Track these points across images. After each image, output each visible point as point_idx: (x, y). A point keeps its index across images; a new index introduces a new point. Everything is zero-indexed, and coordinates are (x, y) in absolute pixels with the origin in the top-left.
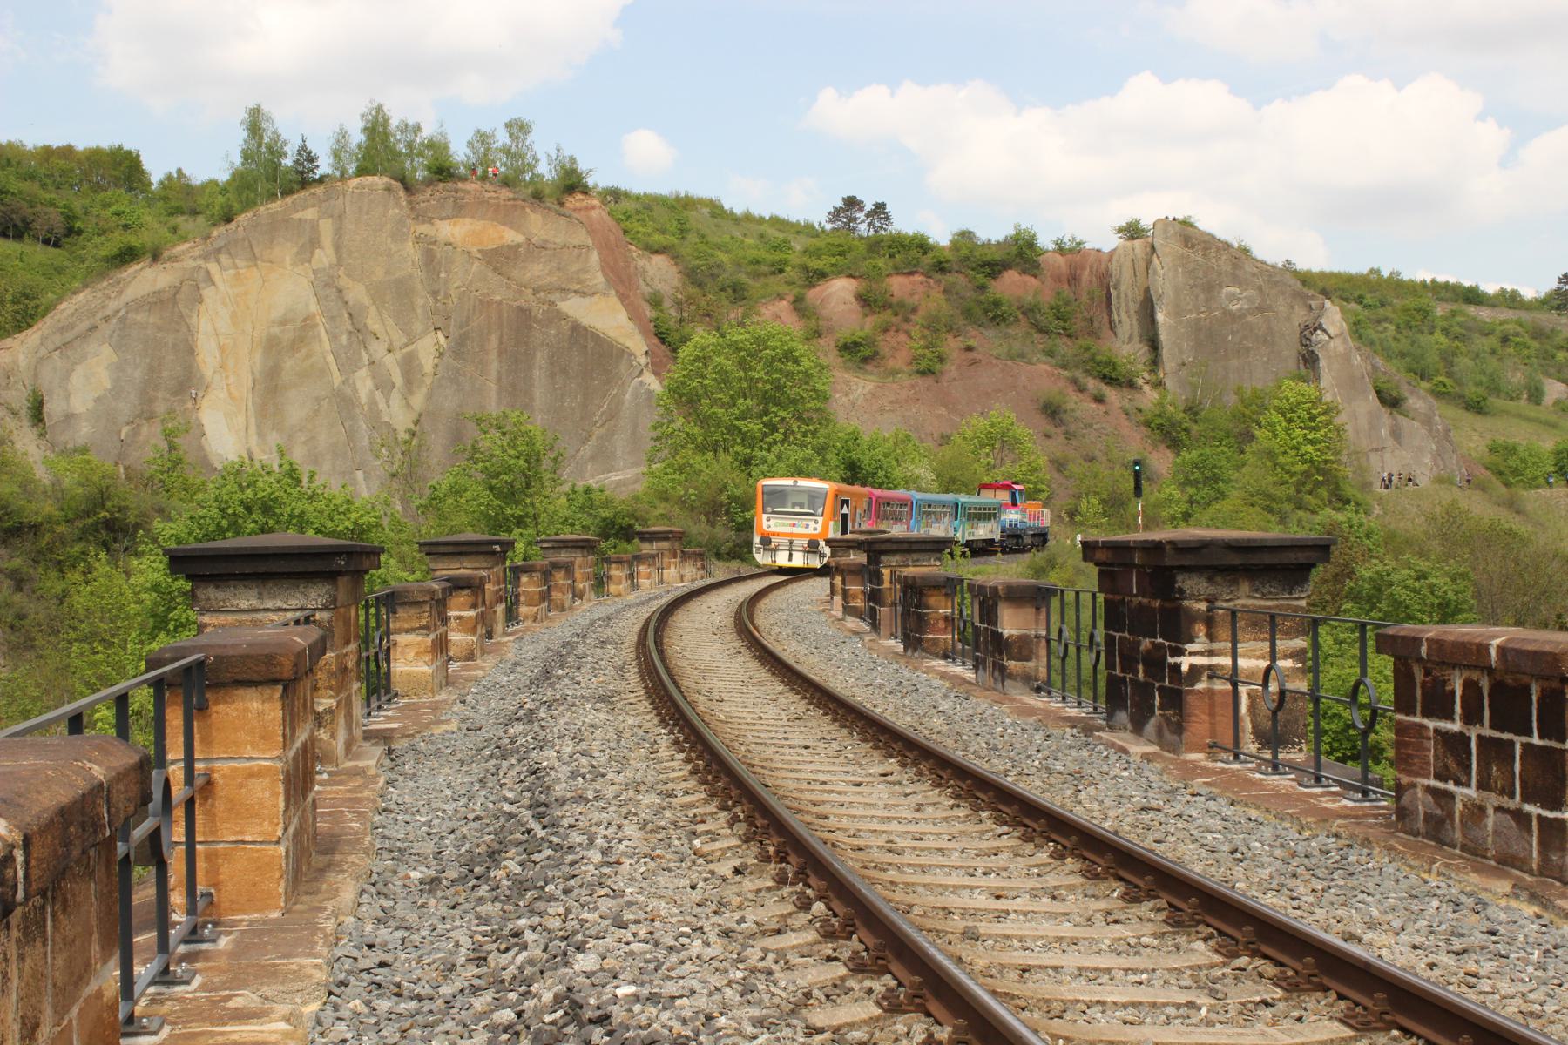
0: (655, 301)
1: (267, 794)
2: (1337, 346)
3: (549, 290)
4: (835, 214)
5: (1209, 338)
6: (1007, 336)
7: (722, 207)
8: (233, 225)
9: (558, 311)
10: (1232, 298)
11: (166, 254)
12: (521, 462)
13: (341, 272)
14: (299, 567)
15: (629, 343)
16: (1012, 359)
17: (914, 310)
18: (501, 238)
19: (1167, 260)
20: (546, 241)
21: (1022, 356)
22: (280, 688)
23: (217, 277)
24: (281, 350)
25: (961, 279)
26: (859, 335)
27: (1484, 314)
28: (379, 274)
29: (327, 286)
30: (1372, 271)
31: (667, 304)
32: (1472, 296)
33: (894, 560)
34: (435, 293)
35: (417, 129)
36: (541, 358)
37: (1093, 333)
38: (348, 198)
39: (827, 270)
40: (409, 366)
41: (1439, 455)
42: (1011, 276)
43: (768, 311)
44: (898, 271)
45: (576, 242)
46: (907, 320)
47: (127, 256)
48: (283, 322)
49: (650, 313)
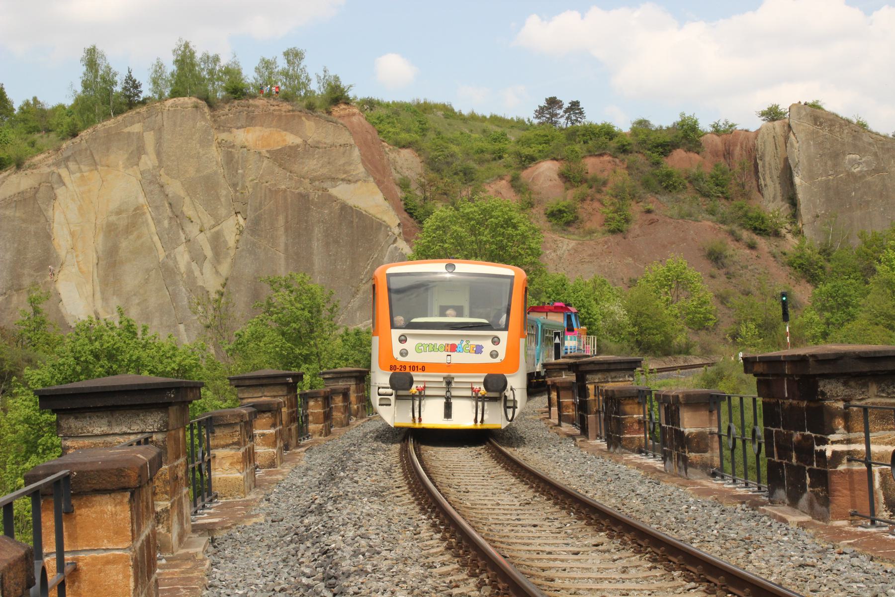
0: (404, 185)
1: (121, 576)
3: (322, 179)
4: (541, 112)
5: (837, 195)
6: (678, 201)
7: (452, 110)
8: (77, 139)
9: (330, 196)
10: (853, 162)
11: (27, 163)
12: (306, 313)
14: (138, 400)
15: (385, 218)
16: (682, 218)
17: (605, 183)
18: (284, 140)
19: (801, 136)
20: (319, 142)
21: (690, 215)
22: (128, 494)
23: (66, 179)
24: (118, 232)
25: (640, 156)
26: (562, 204)
28: (192, 172)
29: (152, 183)
31: (413, 187)
33: (597, 378)
34: (234, 186)
35: (216, 59)
36: (317, 232)
37: (746, 195)
38: (165, 115)
39: (537, 155)
40: (217, 242)
42: (679, 154)
43: (491, 189)
44: (591, 154)
45: (342, 142)
46: (599, 191)
48: (119, 212)
49: (400, 194)
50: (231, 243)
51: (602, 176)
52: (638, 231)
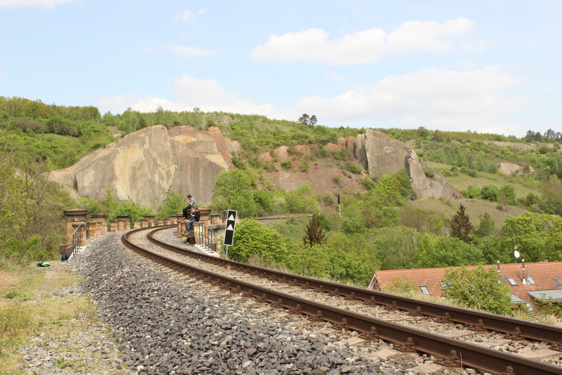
0: (233, 154)
2: (415, 162)
4: (301, 119)
5: (381, 160)
7: (266, 118)
8: (123, 138)
10: (387, 149)
13: (151, 149)
16: (327, 167)
17: (302, 155)
19: (369, 140)
21: (330, 166)
23: (120, 152)
24: (136, 169)
26: (287, 161)
27: (501, 144)
28: (160, 150)
29: (147, 153)
30: (468, 131)
32: (499, 138)
34: (174, 154)
36: (201, 170)
40: (168, 173)
41: (444, 190)
42: (330, 144)
44: (299, 144)
46: (300, 157)
47: (97, 147)
48: (136, 163)
49: (231, 157)
50: (173, 173)
51: (302, 152)
52: (312, 171)
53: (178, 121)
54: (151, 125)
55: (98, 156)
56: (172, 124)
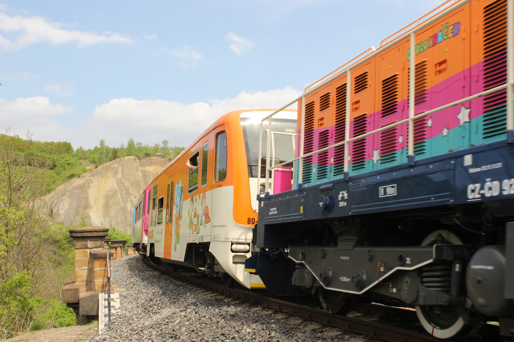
8: (97, 169)
11: (82, 176)
13: (123, 179)
29: (120, 182)
35: (141, 144)
47: (72, 176)
53: (149, 152)
54: (124, 156)
55: (73, 186)
56: (144, 155)
